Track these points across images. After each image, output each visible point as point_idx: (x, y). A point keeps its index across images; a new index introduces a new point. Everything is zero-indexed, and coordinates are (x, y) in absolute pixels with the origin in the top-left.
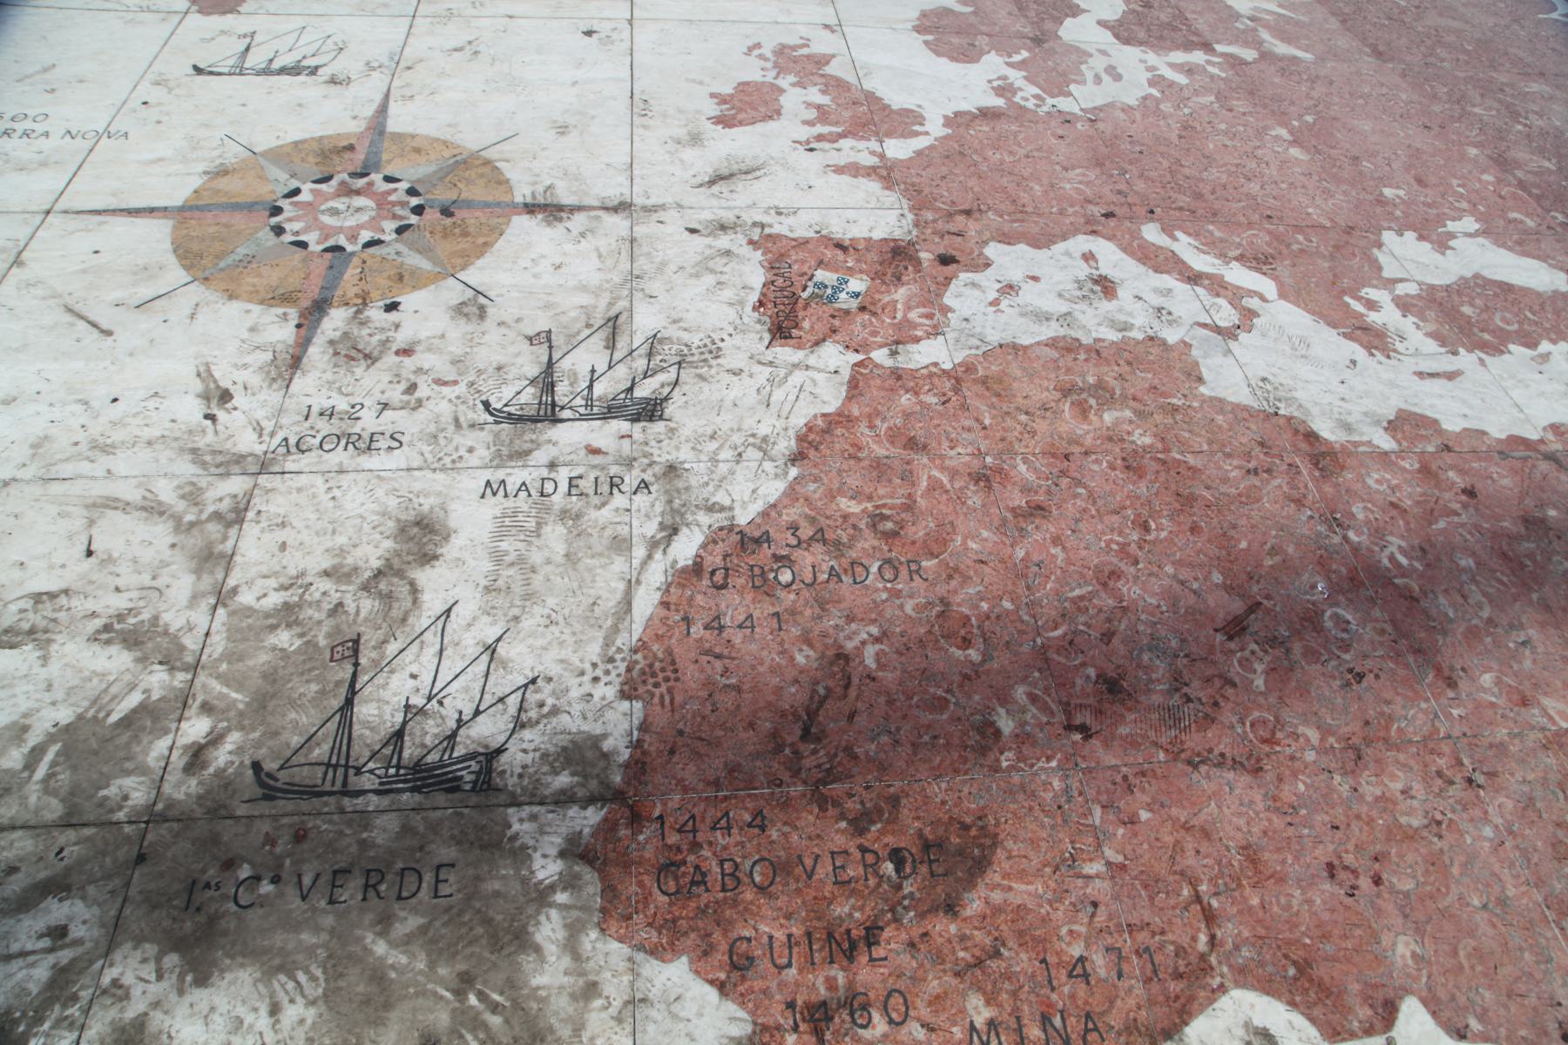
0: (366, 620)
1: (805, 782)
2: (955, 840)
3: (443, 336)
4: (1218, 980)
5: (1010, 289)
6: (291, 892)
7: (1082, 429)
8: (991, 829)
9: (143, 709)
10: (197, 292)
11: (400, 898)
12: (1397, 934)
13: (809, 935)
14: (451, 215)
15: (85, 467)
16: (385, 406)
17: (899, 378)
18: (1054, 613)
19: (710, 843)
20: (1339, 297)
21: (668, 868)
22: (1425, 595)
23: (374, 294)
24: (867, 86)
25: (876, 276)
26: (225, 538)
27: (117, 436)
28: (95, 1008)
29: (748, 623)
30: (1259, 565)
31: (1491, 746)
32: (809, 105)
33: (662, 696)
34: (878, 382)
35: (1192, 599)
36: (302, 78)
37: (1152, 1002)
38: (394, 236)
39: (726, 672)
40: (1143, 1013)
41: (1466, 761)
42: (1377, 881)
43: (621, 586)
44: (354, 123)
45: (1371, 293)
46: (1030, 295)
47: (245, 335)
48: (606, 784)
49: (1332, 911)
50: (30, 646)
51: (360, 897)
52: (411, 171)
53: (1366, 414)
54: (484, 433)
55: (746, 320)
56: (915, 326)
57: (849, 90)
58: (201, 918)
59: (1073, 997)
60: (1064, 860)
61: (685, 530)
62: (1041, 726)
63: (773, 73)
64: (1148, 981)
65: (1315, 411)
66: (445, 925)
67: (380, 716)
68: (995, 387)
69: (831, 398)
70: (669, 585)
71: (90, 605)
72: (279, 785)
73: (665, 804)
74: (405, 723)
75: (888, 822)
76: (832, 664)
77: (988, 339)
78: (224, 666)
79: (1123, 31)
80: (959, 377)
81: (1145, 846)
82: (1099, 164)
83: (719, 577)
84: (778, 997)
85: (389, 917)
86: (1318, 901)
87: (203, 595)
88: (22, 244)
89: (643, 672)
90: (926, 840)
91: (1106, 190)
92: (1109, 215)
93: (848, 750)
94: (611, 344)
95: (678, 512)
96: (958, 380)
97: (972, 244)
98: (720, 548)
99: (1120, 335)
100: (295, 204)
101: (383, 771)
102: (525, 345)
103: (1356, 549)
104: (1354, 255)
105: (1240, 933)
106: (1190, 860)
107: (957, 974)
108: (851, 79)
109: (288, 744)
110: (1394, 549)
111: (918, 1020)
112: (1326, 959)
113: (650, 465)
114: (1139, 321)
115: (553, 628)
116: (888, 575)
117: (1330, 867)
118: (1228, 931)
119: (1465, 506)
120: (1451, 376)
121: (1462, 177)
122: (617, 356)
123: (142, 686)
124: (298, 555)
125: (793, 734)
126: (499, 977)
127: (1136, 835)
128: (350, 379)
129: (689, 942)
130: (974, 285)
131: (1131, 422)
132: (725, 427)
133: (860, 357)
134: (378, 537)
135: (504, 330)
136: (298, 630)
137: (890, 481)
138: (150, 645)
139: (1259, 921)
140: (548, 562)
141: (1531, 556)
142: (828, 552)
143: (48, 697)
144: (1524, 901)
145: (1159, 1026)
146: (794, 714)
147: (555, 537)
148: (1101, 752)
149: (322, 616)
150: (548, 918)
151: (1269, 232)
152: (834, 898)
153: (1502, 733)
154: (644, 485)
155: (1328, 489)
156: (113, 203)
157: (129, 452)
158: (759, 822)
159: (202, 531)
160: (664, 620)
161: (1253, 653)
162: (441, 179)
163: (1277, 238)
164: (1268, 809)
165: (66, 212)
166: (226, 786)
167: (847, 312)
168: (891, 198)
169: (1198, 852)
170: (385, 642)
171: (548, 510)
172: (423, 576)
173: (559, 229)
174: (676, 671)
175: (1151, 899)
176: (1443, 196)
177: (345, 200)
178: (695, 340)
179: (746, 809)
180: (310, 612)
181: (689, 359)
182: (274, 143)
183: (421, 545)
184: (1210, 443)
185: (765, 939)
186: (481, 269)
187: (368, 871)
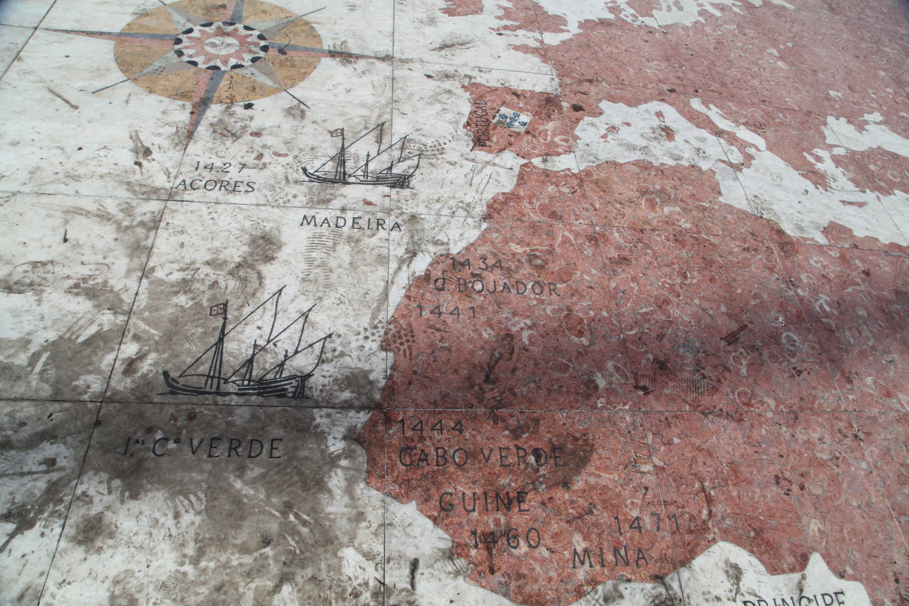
0: (231, 292)
1: (486, 407)
2: (570, 446)
3: (279, 127)
4: (712, 536)
5: (613, 129)
6: (186, 449)
7: (651, 215)
8: (590, 441)
9: (98, 335)
10: (129, 87)
11: (250, 456)
12: (811, 518)
13: (485, 494)
14: (285, 53)
15: (62, 188)
16: (244, 166)
17: (547, 176)
19: (431, 438)
20: (801, 153)
21: (405, 450)
22: (838, 328)
23: (238, 98)
25: (536, 114)
26: (147, 238)
27: (82, 171)
29: (456, 312)
30: (747, 304)
31: (869, 418)
32: (500, 7)
33: (405, 351)
35: (709, 320)
37: (675, 545)
38: (250, 63)
39: (442, 339)
40: (670, 551)
41: (854, 425)
42: (802, 488)
43: (383, 284)
45: (819, 152)
47: (160, 116)
49: (777, 502)
50: (31, 293)
51: (227, 454)
52: (261, 24)
53: (812, 222)
54: (303, 187)
55: (459, 133)
56: (558, 146)
58: (134, 460)
59: (631, 539)
60: (630, 462)
61: (420, 255)
62: (621, 385)
64: (673, 533)
65: (783, 218)
66: (276, 474)
67: (239, 350)
68: (602, 186)
69: (508, 184)
70: (411, 286)
71: (66, 271)
72: (179, 386)
73: (405, 413)
74: (254, 355)
75: (533, 433)
76: (503, 339)
77: (600, 157)
78: (147, 314)
80: (582, 178)
81: (676, 458)
82: (668, 60)
83: (440, 283)
84: (467, 528)
85: (243, 467)
86: (769, 496)
87: (134, 270)
88: (20, 46)
89: (394, 336)
90: (554, 445)
91: (671, 76)
92: (672, 91)
93: (511, 390)
94: (379, 140)
95: (417, 243)
96: (581, 180)
97: (592, 100)
98: (441, 267)
99: (675, 163)
100: (190, 38)
101: (240, 383)
102: (328, 136)
103: (801, 300)
104: (810, 128)
105: (725, 511)
106: (700, 468)
107: (568, 522)
109: (184, 362)
110: (822, 301)
111: (545, 546)
115: (342, 306)
116: (537, 291)
117: (777, 477)
118: (719, 509)
119: (863, 281)
120: (861, 205)
121: (875, 88)
122: (383, 148)
123: (98, 322)
125: (480, 379)
126: (307, 506)
127: (671, 451)
128: (222, 148)
129: (417, 494)
130: (593, 124)
131: (679, 214)
132: (446, 196)
133: (525, 161)
134: (239, 244)
135: (315, 126)
136: (191, 295)
137: (540, 236)
138: (102, 298)
139: (736, 505)
140: (340, 266)
141: (897, 313)
142: (503, 274)
144: (881, 505)
145: (678, 559)
146: (480, 367)
147: (344, 252)
148: (653, 403)
150: (336, 474)
151: (763, 110)
152: (501, 474)
153: (875, 411)
154: (397, 226)
155: (788, 263)
156: (77, 27)
157: (89, 181)
158: (459, 428)
159: (133, 232)
160: (407, 306)
161: (741, 353)
162: (279, 31)
163: (767, 114)
164: (745, 443)
165: (47, 29)
166: (148, 384)
167: (518, 134)
168: (546, 68)
170: (242, 306)
171: (340, 236)
172: (265, 269)
173: (349, 69)
174: (413, 336)
175: (678, 487)
176: (863, 98)
178: (429, 142)
179: (452, 419)
180: (198, 285)
181: (425, 153)
183: (265, 251)
184: (724, 230)
185: (460, 495)
186: (303, 88)
187: (232, 440)
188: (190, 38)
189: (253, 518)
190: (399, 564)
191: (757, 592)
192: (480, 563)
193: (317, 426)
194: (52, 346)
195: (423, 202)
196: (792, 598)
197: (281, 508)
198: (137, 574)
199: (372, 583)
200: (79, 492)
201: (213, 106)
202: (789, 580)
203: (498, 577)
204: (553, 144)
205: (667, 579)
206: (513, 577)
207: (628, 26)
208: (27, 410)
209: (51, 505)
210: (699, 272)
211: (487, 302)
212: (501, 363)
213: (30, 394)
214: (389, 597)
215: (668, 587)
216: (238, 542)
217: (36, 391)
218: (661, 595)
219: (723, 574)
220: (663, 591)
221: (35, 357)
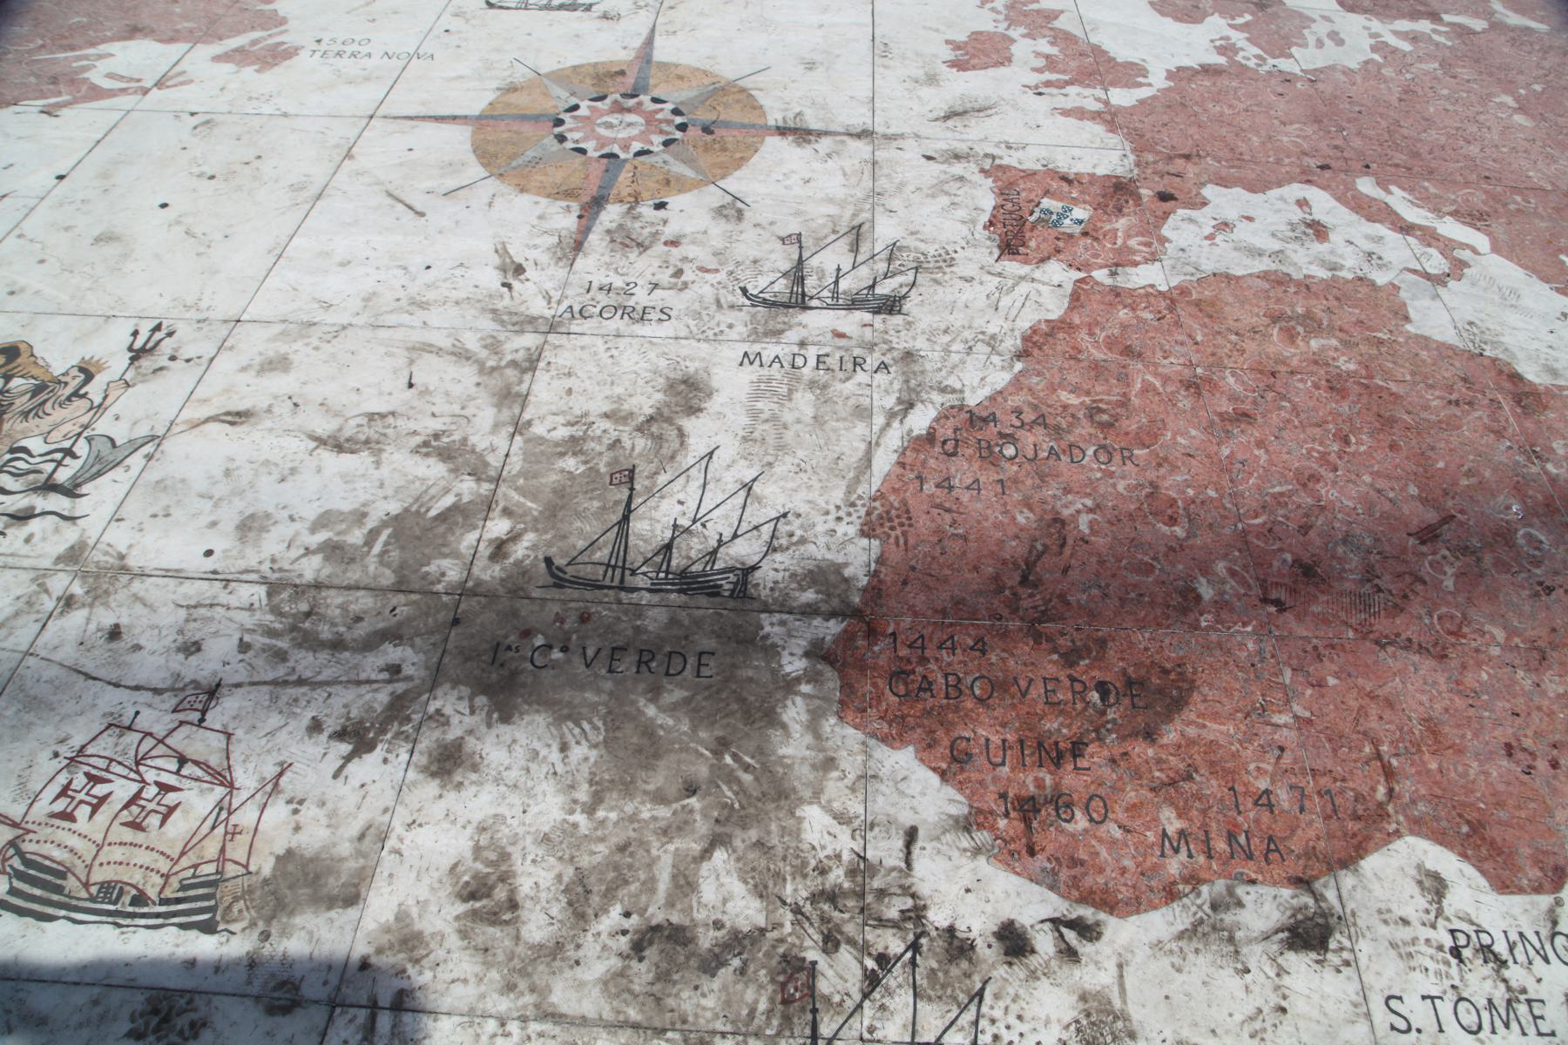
0: (640, 455)
1: (1022, 619)
2: (1156, 681)
3: (705, 232)
5: (1225, 226)
6: (577, 661)
9: (455, 508)
10: (493, 185)
11: (667, 674)
13: (1021, 742)
14: (712, 133)
15: (405, 318)
16: (656, 286)
17: (1118, 295)
18: (1255, 504)
19: (937, 660)
23: (645, 194)
24: (1094, 40)
26: (521, 382)
27: (431, 295)
28: (424, 729)
30: (1455, 484)
32: (1038, 54)
33: (897, 538)
34: (1098, 297)
36: (578, 14)
37: (1331, 836)
39: (954, 523)
40: (1322, 844)
42: (1555, 765)
43: (863, 446)
46: (1243, 232)
47: (535, 222)
48: (846, 602)
49: (1508, 784)
52: (676, 94)
55: (977, 236)
56: (1134, 252)
58: (504, 672)
59: (1257, 821)
60: (1255, 709)
61: (920, 405)
63: (1005, 25)
64: (1327, 818)
65: (1520, 355)
66: (706, 699)
67: (652, 531)
69: (1055, 308)
70: (905, 449)
71: (412, 426)
73: (897, 624)
74: (673, 539)
75: (1096, 659)
76: (1049, 526)
78: (521, 481)
80: (1173, 298)
82: (1318, 121)
83: (950, 446)
87: (504, 424)
91: (1323, 145)
92: (1323, 167)
94: (855, 248)
96: (1173, 301)
97: (1190, 184)
98: (951, 423)
99: (1330, 274)
100: (575, 118)
102: (778, 244)
103: (1553, 480)
105: (1416, 791)
106: (1373, 723)
107: (1152, 790)
108: (1078, 33)
112: (1500, 823)
113: (891, 349)
114: (1349, 263)
115: (802, 475)
118: (1405, 787)
122: (860, 259)
123: (455, 490)
125: (1013, 579)
126: (751, 745)
127: (1323, 696)
130: (1191, 220)
131: (1336, 349)
132: (958, 324)
133: (1082, 275)
135: (759, 230)
140: (798, 421)
142: (1049, 435)
143: (381, 493)
147: (805, 402)
148: (1293, 624)
149: (603, 449)
151: (1486, 192)
154: (884, 366)
155: (1529, 424)
158: (981, 647)
160: (900, 477)
161: (1444, 557)
162: (702, 102)
163: (1494, 197)
164: (1451, 691)
166: (524, 573)
167: (1071, 236)
168: (1114, 140)
169: (1381, 718)
171: (798, 380)
172: (689, 424)
173: (807, 151)
175: (1335, 751)
177: (619, 116)
178: (931, 250)
180: (592, 445)
182: (555, 67)
184: (1413, 374)
185: (982, 741)
186: (739, 179)
188: (575, 118)
189: (673, 757)
191: (1474, 918)
192: (1013, 839)
193: (766, 637)
194: (396, 522)
196: (1537, 933)
197: (714, 745)
198: (509, 821)
199: (846, 856)
200: (431, 709)
202: (1532, 903)
203: (1040, 861)
204: (1125, 248)
205: (1317, 885)
207: (1249, 74)
208: (363, 602)
209: (396, 724)
210: (1371, 435)
211: (1023, 472)
212: (1045, 559)
213: (366, 581)
214: (872, 877)
215: (1318, 898)
216: (651, 787)
217: (375, 577)
218: (1306, 907)
219: (1414, 884)
220: (1310, 901)
221: (373, 535)
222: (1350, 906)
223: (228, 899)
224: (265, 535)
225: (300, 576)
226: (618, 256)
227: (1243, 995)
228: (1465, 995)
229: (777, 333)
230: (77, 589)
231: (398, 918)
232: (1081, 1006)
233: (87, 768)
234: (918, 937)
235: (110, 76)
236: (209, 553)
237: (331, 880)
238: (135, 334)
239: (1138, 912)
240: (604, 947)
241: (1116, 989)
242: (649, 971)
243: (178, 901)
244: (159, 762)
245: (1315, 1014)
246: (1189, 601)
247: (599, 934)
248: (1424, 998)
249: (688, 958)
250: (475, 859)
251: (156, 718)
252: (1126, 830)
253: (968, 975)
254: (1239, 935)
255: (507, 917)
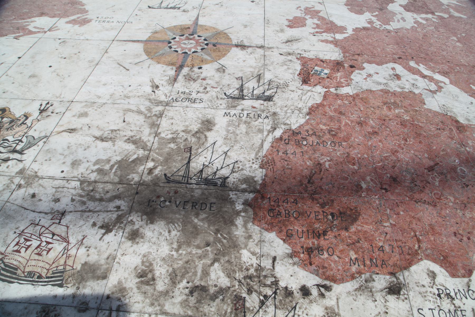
0: (193, 143)
1: (308, 194)
2: (349, 213)
4: (420, 257)
5: (370, 75)
6: (174, 205)
7: (389, 113)
9: (137, 159)
10: (150, 61)
11: (201, 209)
13: (308, 231)
14: (216, 46)
15: (123, 101)
16: (198, 92)
17: (338, 96)
18: (379, 159)
19: (282, 206)
23: (195, 65)
24: (331, 19)
26: (157, 121)
27: (130, 94)
28: (127, 225)
29: (294, 153)
30: (439, 153)
32: (314, 23)
33: (271, 169)
36: (176, 10)
37: (401, 260)
39: (288, 164)
40: (399, 262)
42: (469, 239)
43: (261, 141)
44: (190, 22)
46: (375, 77)
47: (162, 72)
48: (255, 188)
49: (455, 244)
52: (205, 34)
55: (295, 78)
56: (343, 83)
57: (325, 20)
58: (152, 208)
59: (379, 255)
61: (278, 129)
63: (304, 14)
64: (400, 254)
65: (459, 115)
66: (212, 217)
67: (197, 166)
69: (319, 100)
70: (273, 142)
71: (124, 134)
73: (271, 195)
74: (203, 168)
75: (330, 206)
76: (317, 165)
77: (363, 88)
78: (157, 151)
79: (407, 8)
80: (354, 97)
82: (398, 44)
83: (287, 141)
87: (152, 133)
89: (266, 162)
91: (399, 51)
92: (400, 58)
93: (320, 187)
94: (259, 81)
96: (354, 98)
97: (359, 63)
98: (287, 134)
100: (175, 41)
102: (236, 80)
103: (468, 153)
106: (414, 226)
107: (347, 245)
108: (326, 17)
109: (173, 171)
112: (452, 256)
113: (269, 112)
118: (424, 245)
122: (260, 84)
123: (137, 153)
124: (176, 126)
126: (226, 231)
127: (399, 218)
128: (189, 85)
130: (360, 74)
132: (289, 104)
133: (327, 90)
135: (230, 76)
139: (433, 244)
140: (241, 133)
142: (317, 138)
147: (243, 127)
149: (182, 141)
151: (448, 66)
154: (267, 117)
155: (461, 136)
158: (296, 202)
160: (272, 150)
161: (436, 176)
162: (213, 37)
166: (158, 179)
167: (324, 78)
168: (337, 49)
169: (416, 224)
170: (198, 149)
171: (241, 121)
172: (208, 134)
173: (244, 52)
174: (274, 163)
175: (402, 234)
177: (188, 41)
178: (282, 82)
180: (179, 140)
182: (169, 26)
184: (426, 120)
187: (193, 202)
188: (175, 41)
189: (202, 235)
190: (267, 258)
191: (444, 285)
192: (305, 260)
193: (231, 198)
194: (119, 162)
195: (279, 107)
196: (464, 290)
198: (153, 254)
199: (255, 265)
200: (129, 219)
201: (185, 68)
202: (462, 281)
203: (313, 267)
204: (340, 82)
205: (397, 275)
206: (321, 268)
207: (377, 30)
208: (109, 187)
209: (119, 224)
210: (414, 139)
212: (315, 175)
213: (110, 180)
214: (262, 272)
215: (397, 279)
216: (196, 244)
217: (113, 179)
218: (394, 281)
220: (395, 280)
221: (112, 167)
222: (407, 281)
223: (67, 277)
224: (79, 166)
225: (90, 179)
226: (187, 83)
227: (375, 308)
228: (442, 308)
229: (235, 107)
230: (22, 182)
231: (118, 283)
232: (326, 311)
233: (24, 237)
234: (276, 290)
235: (35, 27)
236: (62, 172)
237: (98, 271)
238: (41, 105)
239: (343, 283)
240: (181, 292)
241: (336, 306)
242: (194, 300)
243: (52, 277)
244: (47, 235)
245: (396, 314)
246: (359, 188)
247: (179, 288)
248: (429, 309)
249: (206, 296)
250: (142, 265)
251: (45, 222)
252: (339, 258)
253: (291, 302)
254: (373, 290)
255: (152, 283)
